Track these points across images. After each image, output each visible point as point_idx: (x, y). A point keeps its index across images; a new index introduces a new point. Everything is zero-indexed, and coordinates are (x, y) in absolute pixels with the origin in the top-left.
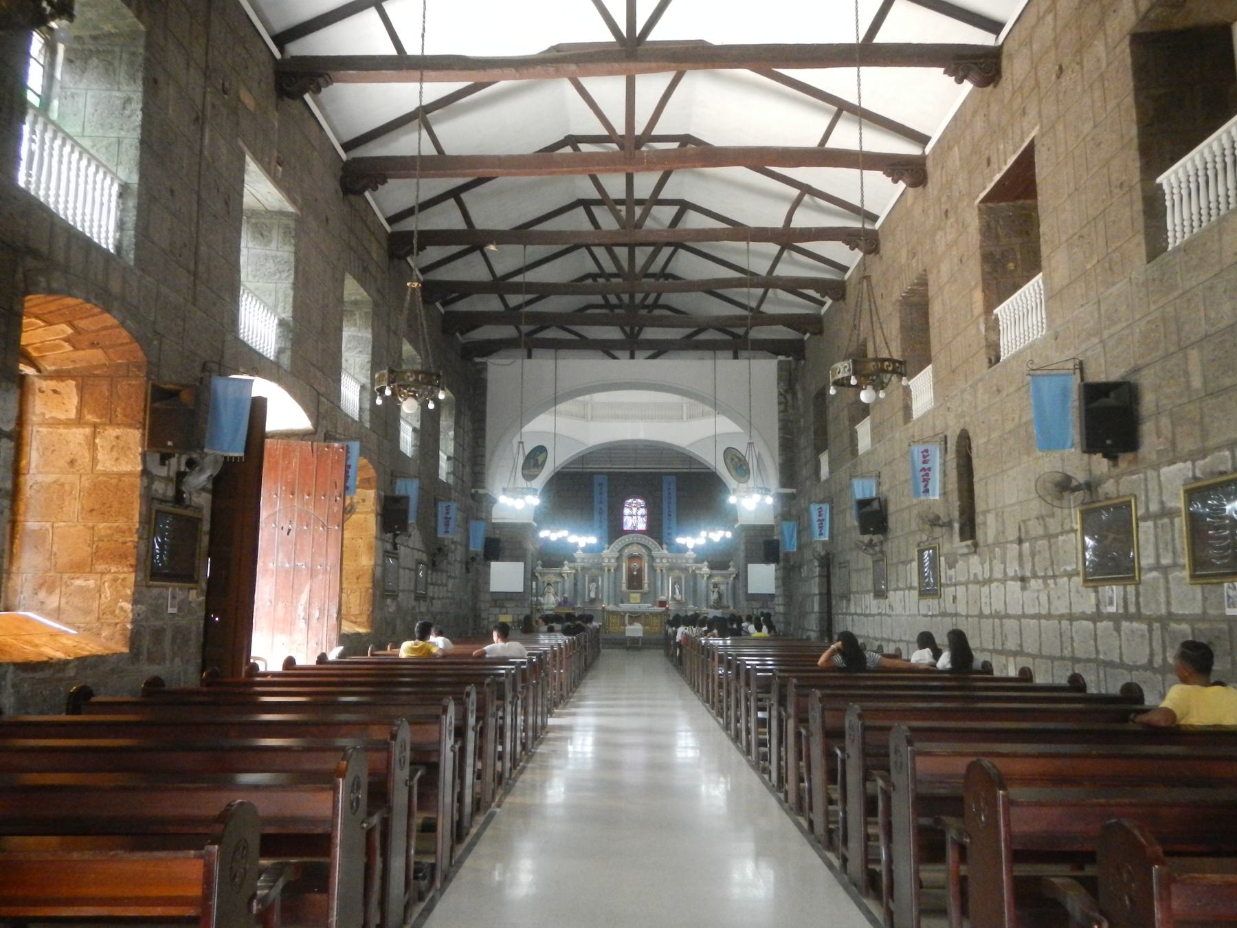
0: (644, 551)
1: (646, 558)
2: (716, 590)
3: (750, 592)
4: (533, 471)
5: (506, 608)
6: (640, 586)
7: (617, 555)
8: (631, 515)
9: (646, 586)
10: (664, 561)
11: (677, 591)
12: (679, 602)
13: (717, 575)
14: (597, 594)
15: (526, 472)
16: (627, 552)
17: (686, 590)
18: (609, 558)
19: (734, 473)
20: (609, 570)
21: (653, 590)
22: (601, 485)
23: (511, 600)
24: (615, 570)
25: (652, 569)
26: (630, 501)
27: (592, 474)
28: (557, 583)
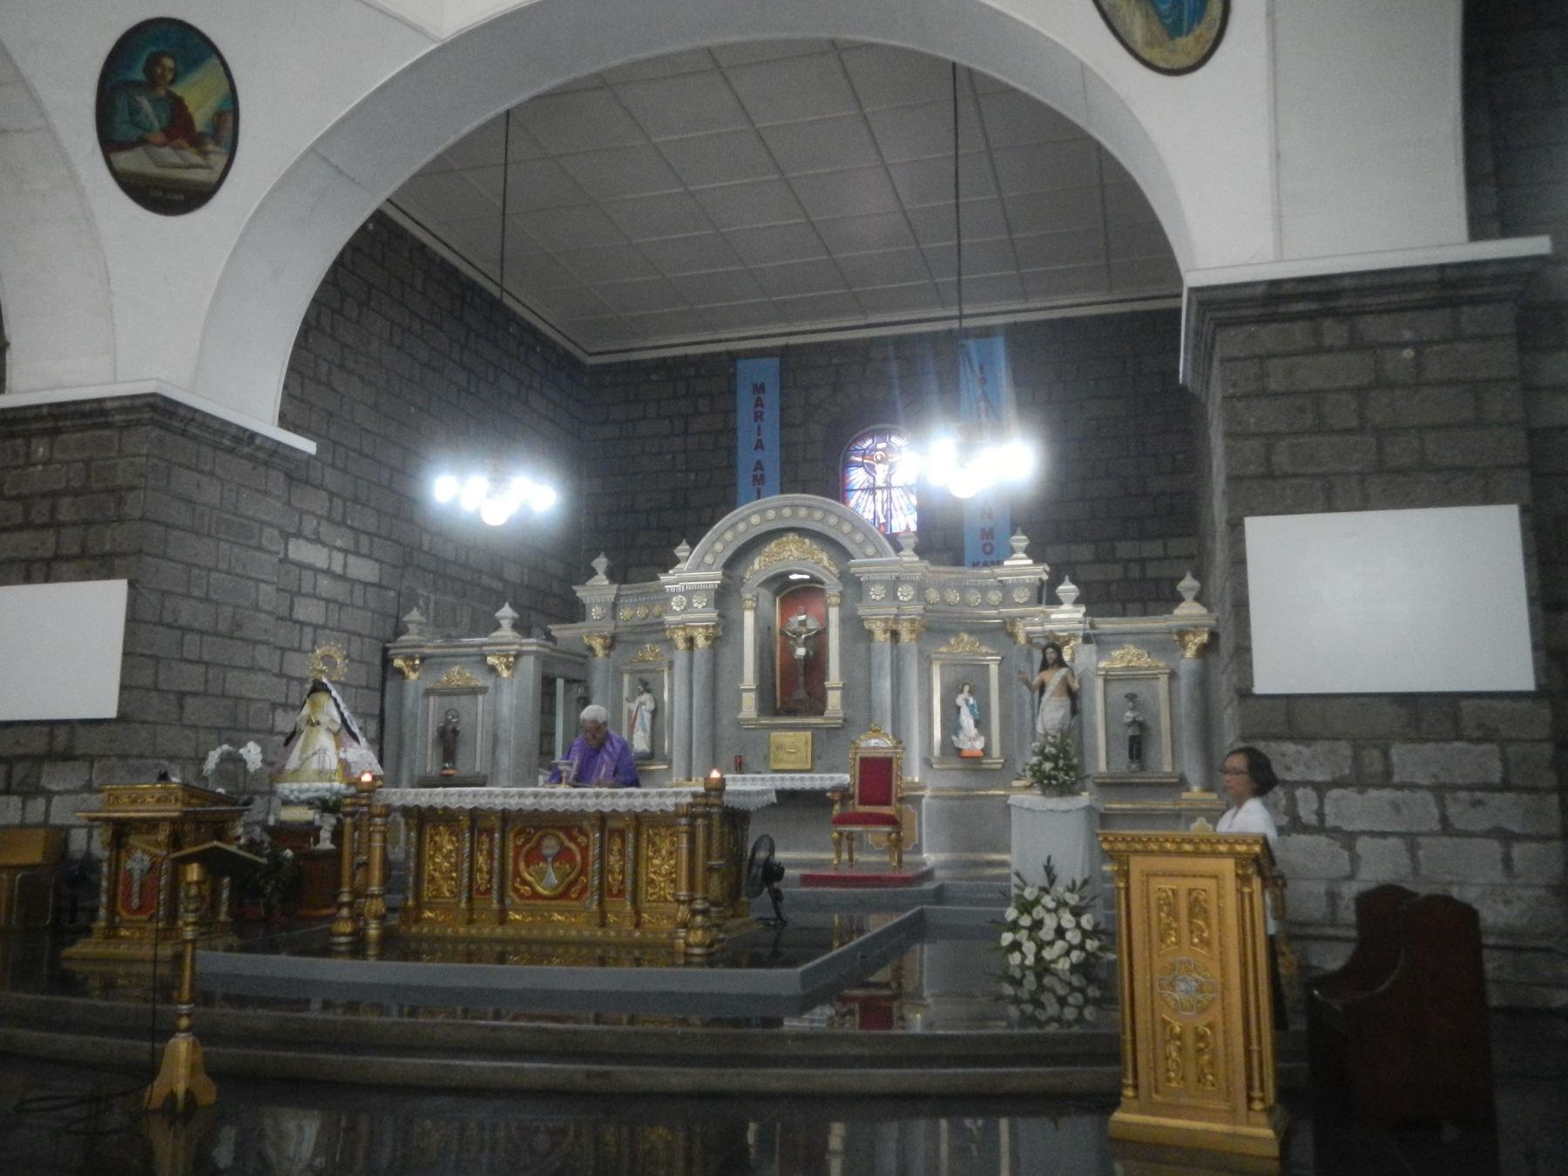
0: (821, 563)
1: (833, 588)
2: (1054, 678)
3: (1266, 682)
4: (171, 162)
5: (49, 795)
6: (818, 706)
7: (714, 577)
8: (872, 490)
9: (834, 699)
10: (905, 593)
11: (967, 720)
12: (974, 764)
13: (1118, 639)
14: (655, 735)
15: (130, 161)
16: (760, 566)
17: (1005, 717)
18: (688, 594)
19: (1137, 27)
20: (691, 641)
21: (861, 714)
22: (759, 388)
23: (67, 756)
24: (715, 641)
25: (857, 631)
26: (869, 442)
27: (733, 356)
28: (474, 692)
